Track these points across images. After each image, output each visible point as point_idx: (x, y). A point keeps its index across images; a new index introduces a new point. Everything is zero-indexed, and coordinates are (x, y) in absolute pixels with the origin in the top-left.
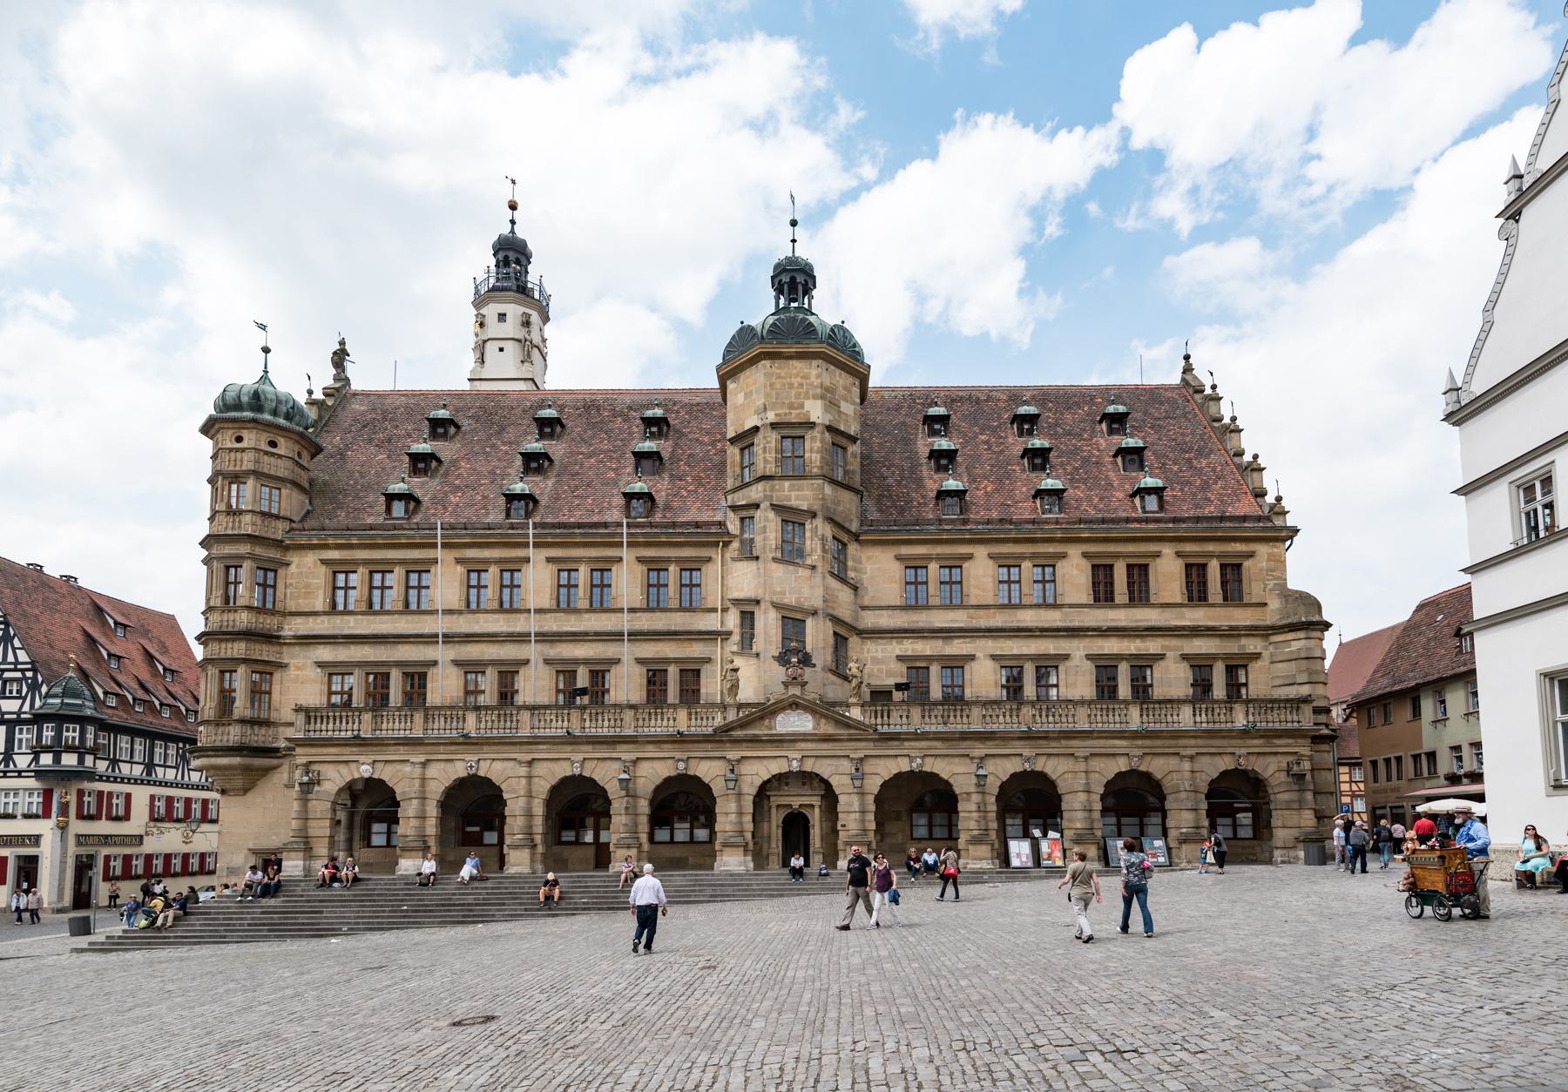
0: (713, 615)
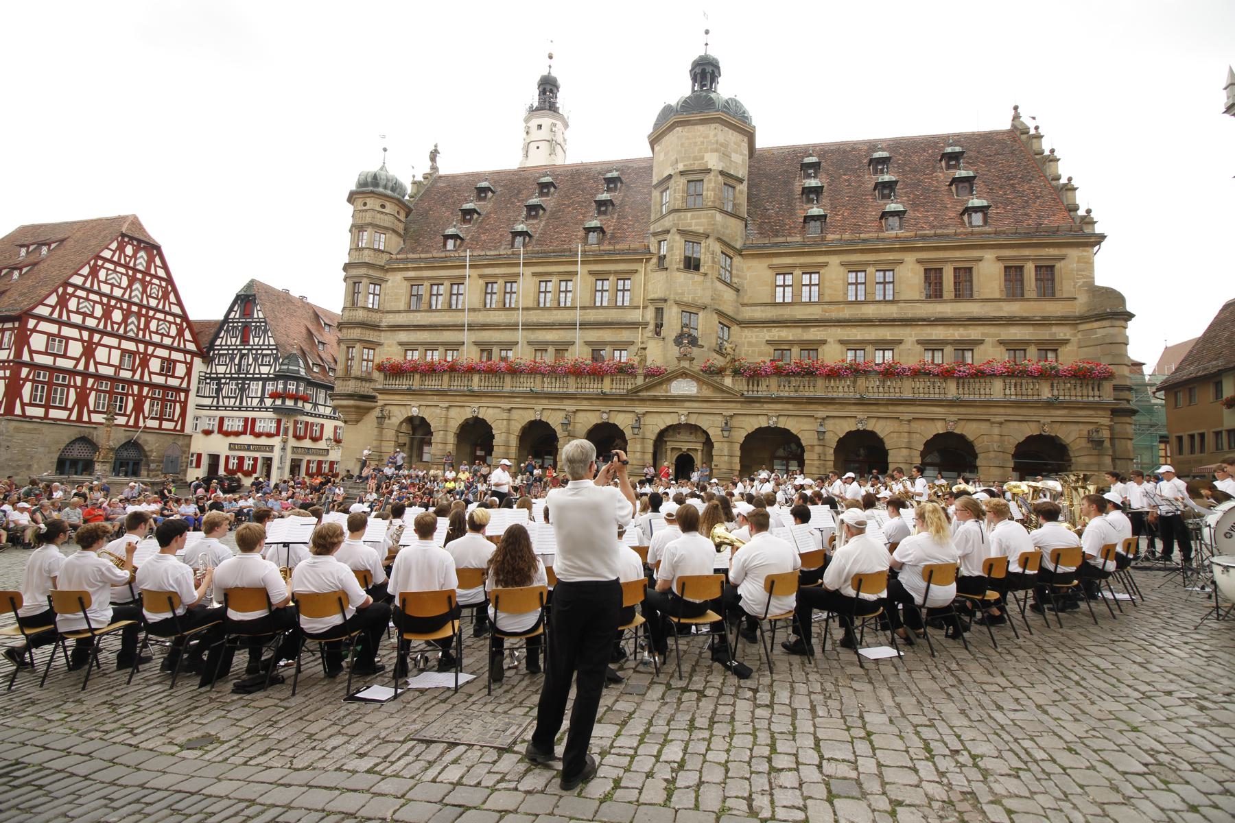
0: (637, 311)
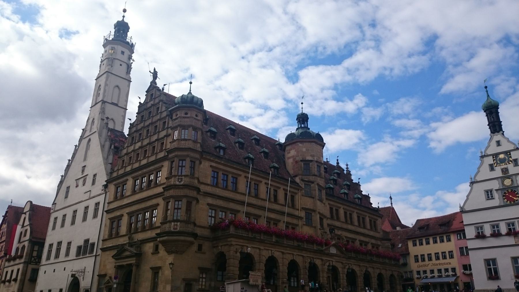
0: (298, 211)
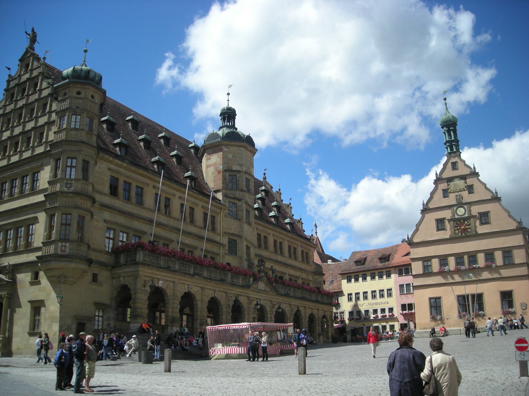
0: (219, 237)
